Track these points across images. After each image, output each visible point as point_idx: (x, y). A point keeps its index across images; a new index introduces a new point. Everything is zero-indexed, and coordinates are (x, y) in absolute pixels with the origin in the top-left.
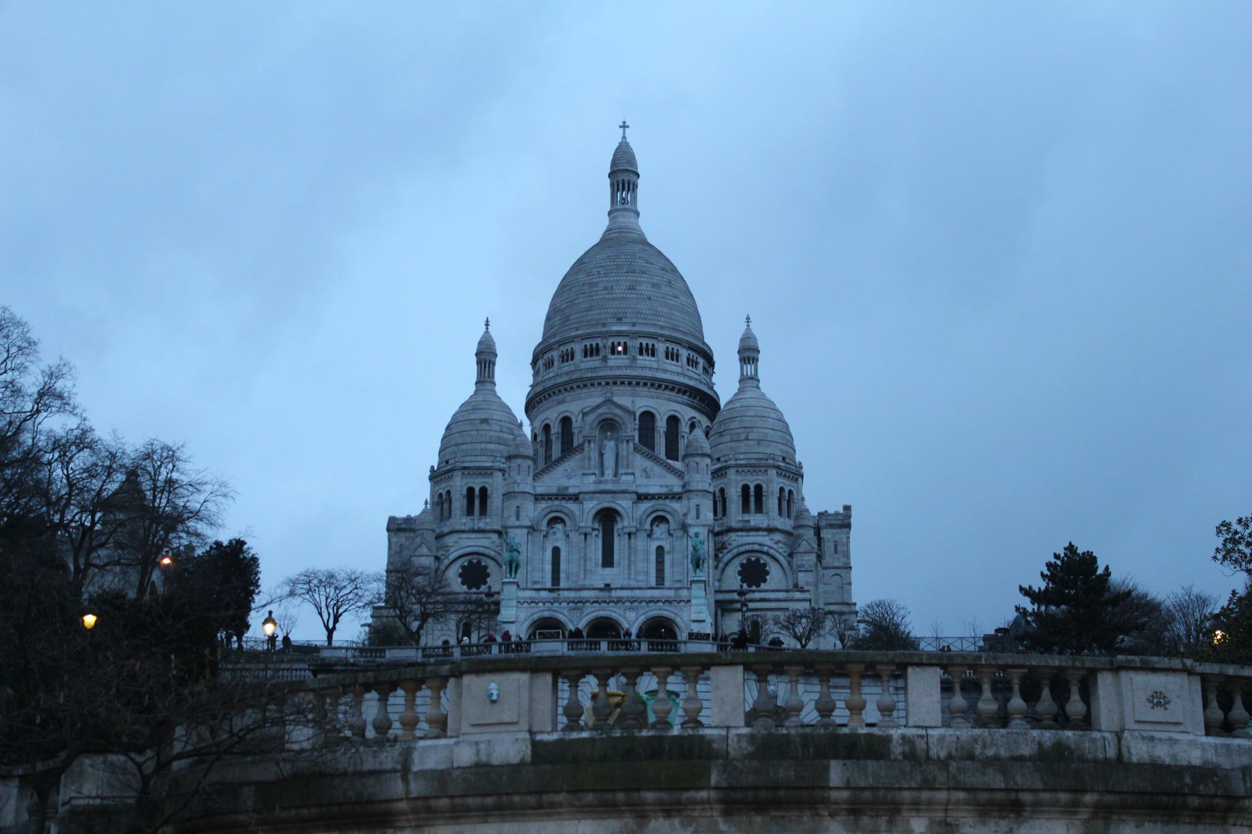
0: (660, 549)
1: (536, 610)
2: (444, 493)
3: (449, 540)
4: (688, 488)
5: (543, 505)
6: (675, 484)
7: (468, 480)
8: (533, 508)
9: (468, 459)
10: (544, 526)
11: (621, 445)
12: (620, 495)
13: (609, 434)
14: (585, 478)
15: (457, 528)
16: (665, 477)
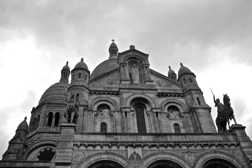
0: (176, 125)
1: (94, 153)
2: (37, 117)
3: (35, 137)
4: (188, 89)
5: (95, 96)
6: (179, 90)
7: (50, 109)
8: (88, 97)
9: (51, 100)
10: (95, 108)
11: (142, 70)
12: (147, 91)
13: (134, 64)
14: (123, 82)
15: (40, 131)
16: (171, 87)
